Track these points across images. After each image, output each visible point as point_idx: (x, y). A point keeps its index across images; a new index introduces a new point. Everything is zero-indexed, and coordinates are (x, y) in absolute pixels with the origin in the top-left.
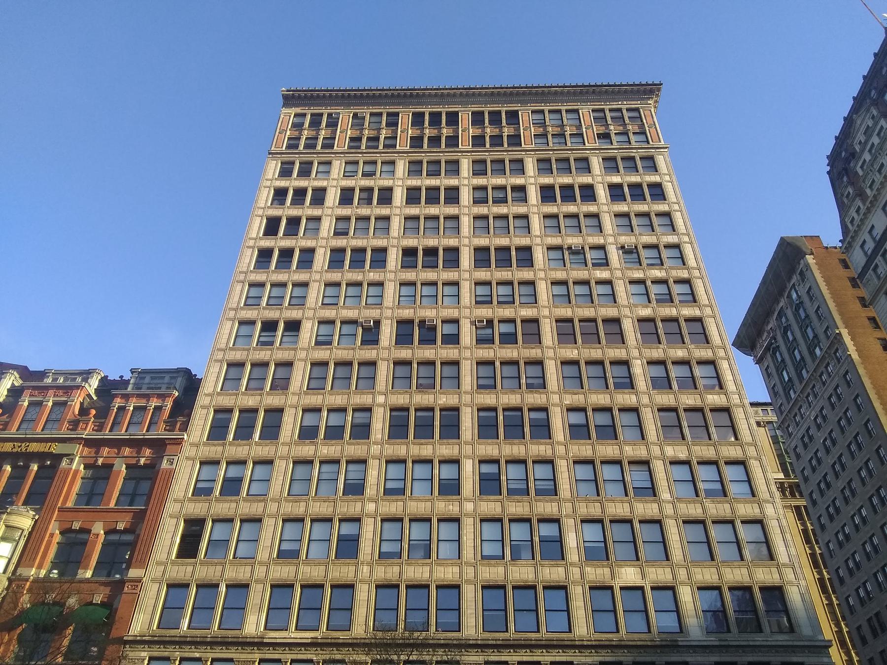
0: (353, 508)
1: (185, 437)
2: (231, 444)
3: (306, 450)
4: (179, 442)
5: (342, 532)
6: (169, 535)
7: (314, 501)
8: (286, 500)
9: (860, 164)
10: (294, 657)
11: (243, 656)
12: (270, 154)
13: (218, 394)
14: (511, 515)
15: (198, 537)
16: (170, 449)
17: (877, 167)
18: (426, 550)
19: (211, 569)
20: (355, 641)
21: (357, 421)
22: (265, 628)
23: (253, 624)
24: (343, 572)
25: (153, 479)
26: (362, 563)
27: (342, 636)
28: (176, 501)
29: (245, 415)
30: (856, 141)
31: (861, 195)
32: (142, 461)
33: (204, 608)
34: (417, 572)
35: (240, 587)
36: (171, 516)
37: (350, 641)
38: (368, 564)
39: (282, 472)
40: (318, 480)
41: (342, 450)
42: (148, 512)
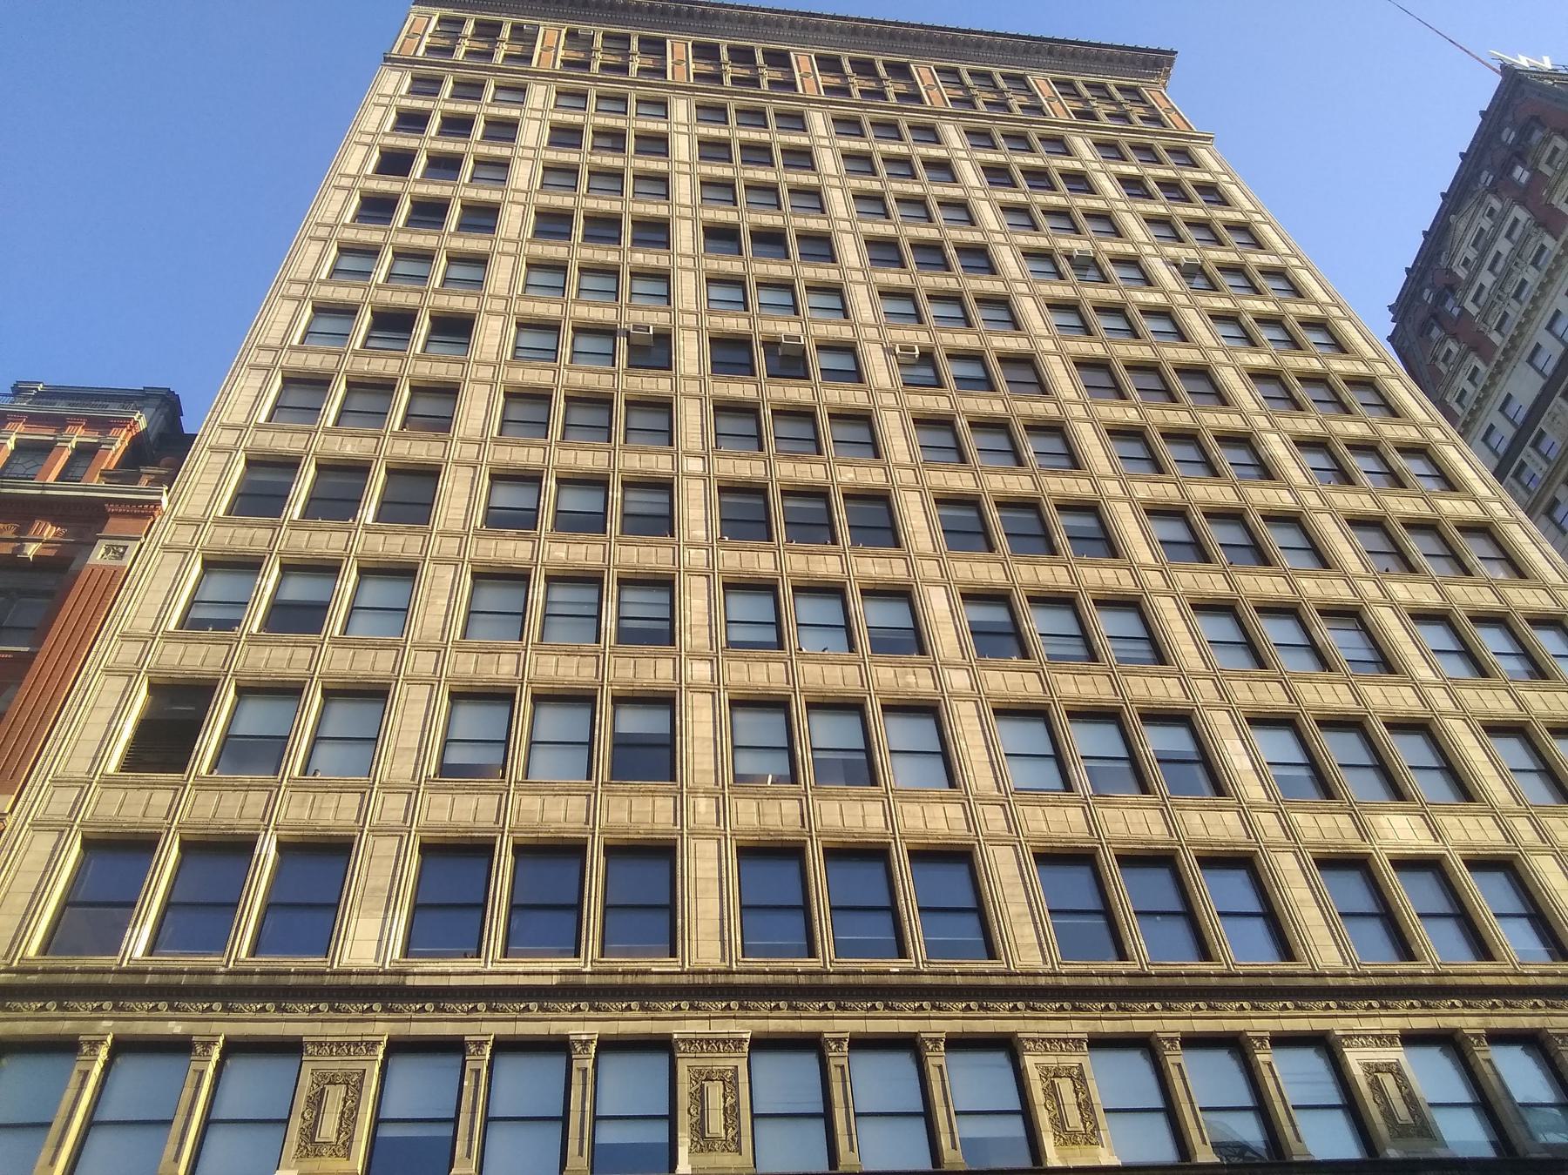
0: (654, 671)
1: (165, 499)
2: (294, 525)
3: (511, 550)
4: (144, 511)
5: (623, 728)
7: (539, 652)
8: (459, 648)
9: (1472, 293)
10: (507, 1029)
11: (335, 1030)
12: (386, 60)
13: (259, 427)
15: (191, 729)
16: (114, 525)
17: (1511, 289)
18: (862, 770)
19: (232, 801)
20: (699, 980)
21: (631, 509)
22: (406, 953)
23: (368, 938)
24: (639, 811)
25: (56, 598)
26: (693, 792)
27: (659, 967)
29: (333, 479)
30: (1459, 260)
31: (1480, 346)
32: (31, 550)
33: (200, 912)
34: (851, 815)
35: (331, 852)
36: (109, 671)
37: (684, 979)
38: (708, 793)
39: (439, 599)
40: (546, 615)
41: (607, 555)
42: (39, 660)
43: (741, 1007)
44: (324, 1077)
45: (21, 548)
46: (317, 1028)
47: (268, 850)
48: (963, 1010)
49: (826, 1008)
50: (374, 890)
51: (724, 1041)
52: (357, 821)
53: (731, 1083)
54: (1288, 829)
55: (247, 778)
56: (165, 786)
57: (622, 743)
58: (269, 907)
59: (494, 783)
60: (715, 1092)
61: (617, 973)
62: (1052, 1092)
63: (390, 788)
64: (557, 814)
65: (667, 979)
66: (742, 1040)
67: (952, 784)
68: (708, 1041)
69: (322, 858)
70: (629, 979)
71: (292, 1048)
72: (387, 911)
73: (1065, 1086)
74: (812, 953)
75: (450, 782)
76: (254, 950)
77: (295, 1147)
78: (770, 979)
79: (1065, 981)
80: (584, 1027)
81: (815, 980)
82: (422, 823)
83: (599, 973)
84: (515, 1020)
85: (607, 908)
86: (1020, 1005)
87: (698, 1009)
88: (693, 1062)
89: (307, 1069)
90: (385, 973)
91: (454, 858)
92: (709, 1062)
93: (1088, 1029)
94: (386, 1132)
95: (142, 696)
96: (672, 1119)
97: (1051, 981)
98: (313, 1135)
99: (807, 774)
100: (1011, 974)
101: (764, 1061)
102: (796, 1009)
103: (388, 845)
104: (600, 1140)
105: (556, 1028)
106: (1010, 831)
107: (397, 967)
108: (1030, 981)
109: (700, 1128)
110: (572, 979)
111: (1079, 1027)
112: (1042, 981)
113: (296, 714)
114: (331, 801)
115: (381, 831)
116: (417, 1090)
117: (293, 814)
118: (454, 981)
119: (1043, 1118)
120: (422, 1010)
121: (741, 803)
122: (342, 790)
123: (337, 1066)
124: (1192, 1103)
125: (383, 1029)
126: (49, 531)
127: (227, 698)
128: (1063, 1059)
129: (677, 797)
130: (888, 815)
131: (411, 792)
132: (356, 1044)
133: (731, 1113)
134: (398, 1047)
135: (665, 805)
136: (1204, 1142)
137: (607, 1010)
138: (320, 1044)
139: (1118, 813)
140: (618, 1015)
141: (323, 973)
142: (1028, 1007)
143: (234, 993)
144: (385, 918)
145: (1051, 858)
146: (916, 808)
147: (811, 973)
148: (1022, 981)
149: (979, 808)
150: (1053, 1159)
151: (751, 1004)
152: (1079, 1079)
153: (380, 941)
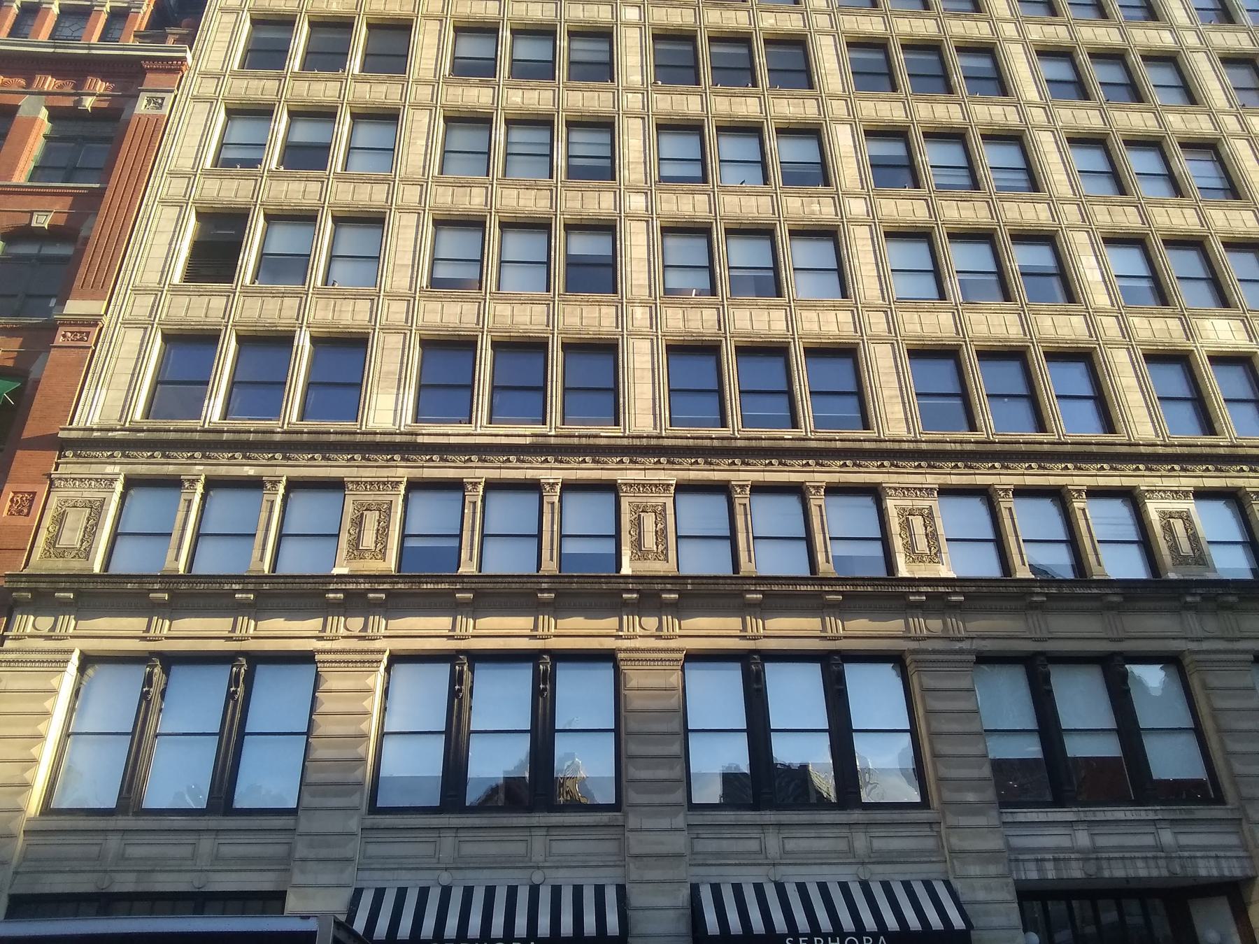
0: (595, 202)
1: (189, 55)
2: (296, 77)
3: (475, 96)
4: (173, 67)
6: (160, 240)
8: (439, 183)
11: (368, 473)
14: (951, 222)
16: (151, 80)
18: (770, 284)
20: (637, 442)
21: (577, 57)
24: (589, 317)
25: (114, 142)
26: (631, 302)
27: (607, 433)
28: (173, 174)
29: (324, 35)
32: (88, 103)
33: (258, 389)
34: (758, 320)
36: (164, 202)
37: (625, 442)
38: (643, 304)
39: (419, 138)
40: (507, 154)
43: (668, 462)
44: (362, 505)
45: (79, 102)
46: (354, 472)
47: (303, 343)
48: (840, 466)
49: (733, 463)
50: (388, 373)
51: (656, 486)
52: (370, 321)
53: (661, 514)
54: (1125, 330)
55: (281, 287)
56: (219, 293)
57: (573, 263)
58: (310, 385)
59: (473, 293)
60: (649, 521)
61: (574, 436)
62: (906, 526)
64: (525, 318)
65: (612, 441)
66: (668, 485)
67: (844, 295)
68: (644, 485)
70: (584, 441)
71: (337, 485)
72: (398, 389)
73: (917, 522)
74: (724, 424)
75: (439, 292)
76: (303, 416)
77: (345, 553)
78: (691, 442)
79: (924, 446)
80: (551, 474)
81: (726, 443)
82: (420, 323)
83: (561, 436)
84: (500, 468)
85: (565, 390)
86: (886, 463)
87: (636, 462)
89: (349, 500)
90: (401, 434)
91: (446, 353)
92: (644, 500)
94: (410, 543)
95: (192, 224)
96: (617, 537)
97: (912, 446)
98: (358, 545)
99: (724, 287)
100: (881, 441)
102: (711, 464)
103: (395, 340)
104: (566, 550)
105: (530, 474)
106: (890, 332)
107: (408, 429)
108: (896, 446)
109: (638, 544)
110: (541, 440)
111: (932, 480)
112: (905, 446)
113: (313, 237)
114: (348, 305)
115: (389, 329)
116: (431, 515)
117: (320, 315)
118: (453, 440)
119: (898, 543)
120: (431, 460)
121: (670, 311)
122: (356, 297)
123: (372, 498)
124: (1017, 536)
125: (403, 473)
126: (100, 86)
127: (258, 225)
128: (915, 502)
129: (619, 306)
130: (790, 320)
132: (384, 483)
133: (661, 535)
134: (415, 486)
135: (609, 313)
136: (1024, 564)
137: (568, 462)
138: (357, 483)
139: (982, 317)
140: (576, 466)
141: (355, 433)
142: (892, 465)
143: (290, 447)
144: (398, 394)
145: (921, 353)
146: (813, 315)
147: (723, 439)
148: (889, 445)
149: (866, 314)
150: (903, 571)
151: (676, 460)
152: (929, 517)
153: (396, 410)
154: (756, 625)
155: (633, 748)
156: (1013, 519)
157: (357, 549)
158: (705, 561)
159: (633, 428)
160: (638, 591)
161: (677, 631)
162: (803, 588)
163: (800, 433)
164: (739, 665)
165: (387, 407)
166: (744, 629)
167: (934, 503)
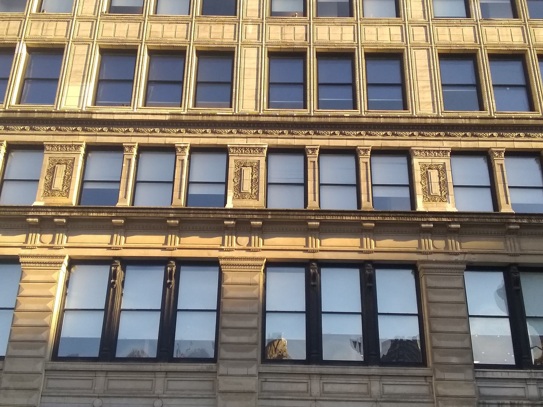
20: (241, 119)
27: (221, 113)
34: (335, 33)
37: (234, 119)
43: (264, 133)
44: (55, 160)
46: (51, 138)
47: (22, 52)
48: (383, 135)
49: (308, 134)
50: (76, 72)
51: (254, 149)
52: (66, 36)
53: (256, 168)
55: (9, 14)
58: (25, 80)
59: (137, 16)
60: (247, 173)
61: (199, 115)
62: (426, 177)
63: (82, 19)
64: (171, 34)
65: (225, 118)
66: (262, 149)
67: (398, 15)
68: (245, 149)
69: (49, 54)
70: (205, 118)
71: (39, 147)
72: (83, 82)
73: (434, 174)
74: (305, 107)
75: (114, 16)
76: (19, 101)
77: (42, 192)
78: (279, 119)
79: (443, 121)
80: (183, 140)
81: (303, 120)
82: (100, 37)
83: (190, 115)
84: (148, 136)
85: (197, 83)
86: (415, 133)
87: (241, 133)
88: (238, 158)
90: (82, 113)
91: (117, 57)
92: (245, 158)
93: (452, 146)
94: (87, 186)
96: (226, 183)
97: (434, 121)
98: (51, 187)
99: (312, 10)
100: (412, 118)
101: (275, 160)
102: (293, 134)
103: (82, 49)
104: (191, 192)
105: (169, 141)
106: (427, 41)
107: (88, 110)
108: (423, 121)
109: (239, 188)
110: (176, 117)
111: (448, 145)
112: (429, 121)
114: (52, 26)
115: (79, 42)
116: (101, 167)
117: (33, 32)
118: (117, 117)
119: (419, 188)
120: (102, 131)
121: (272, 28)
122: (58, 20)
123: (61, 156)
124: (504, 184)
125: (83, 139)
128: (434, 160)
129: (237, 24)
130: (356, 34)
131: (93, 20)
132: (70, 146)
133: (255, 182)
134: (91, 148)
135: (229, 29)
136: (507, 203)
137: (195, 133)
138: (52, 146)
139: (494, 30)
140: (200, 135)
141: (51, 112)
142: (420, 134)
144: (82, 86)
145: (448, 56)
146: (373, 29)
147: (301, 116)
148: (418, 121)
149: (411, 28)
150: (421, 207)
151: (269, 131)
152: (442, 170)
153: (80, 97)
154: (316, 243)
155: (225, 322)
156: (502, 172)
157: (50, 189)
158: (283, 200)
159: (241, 109)
160: (234, 219)
161: (261, 246)
162: (348, 218)
163: (357, 112)
164: (303, 270)
165: (75, 94)
166: (307, 245)
167: (446, 160)
